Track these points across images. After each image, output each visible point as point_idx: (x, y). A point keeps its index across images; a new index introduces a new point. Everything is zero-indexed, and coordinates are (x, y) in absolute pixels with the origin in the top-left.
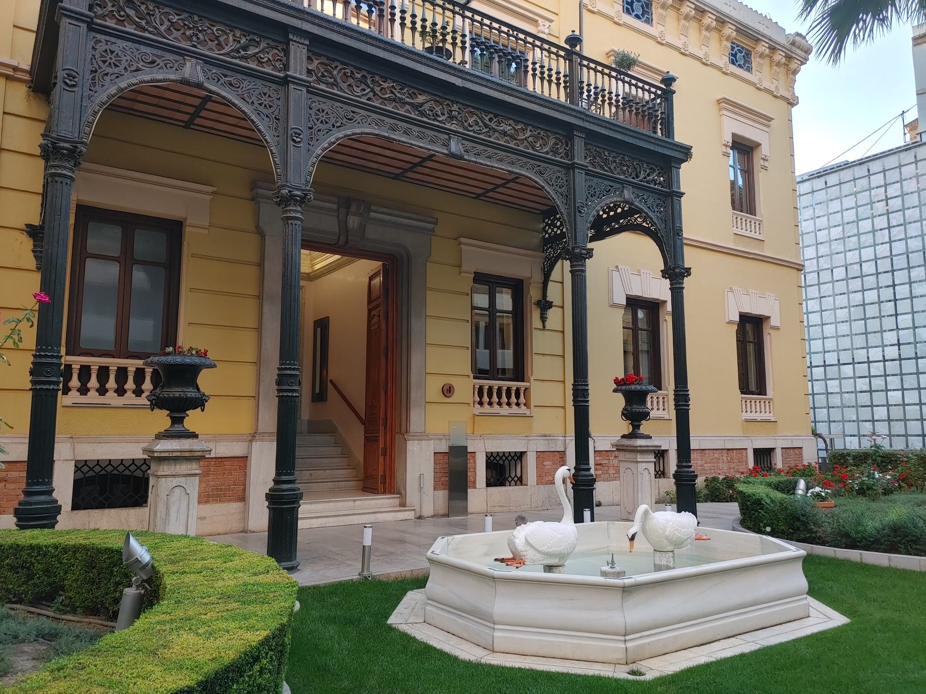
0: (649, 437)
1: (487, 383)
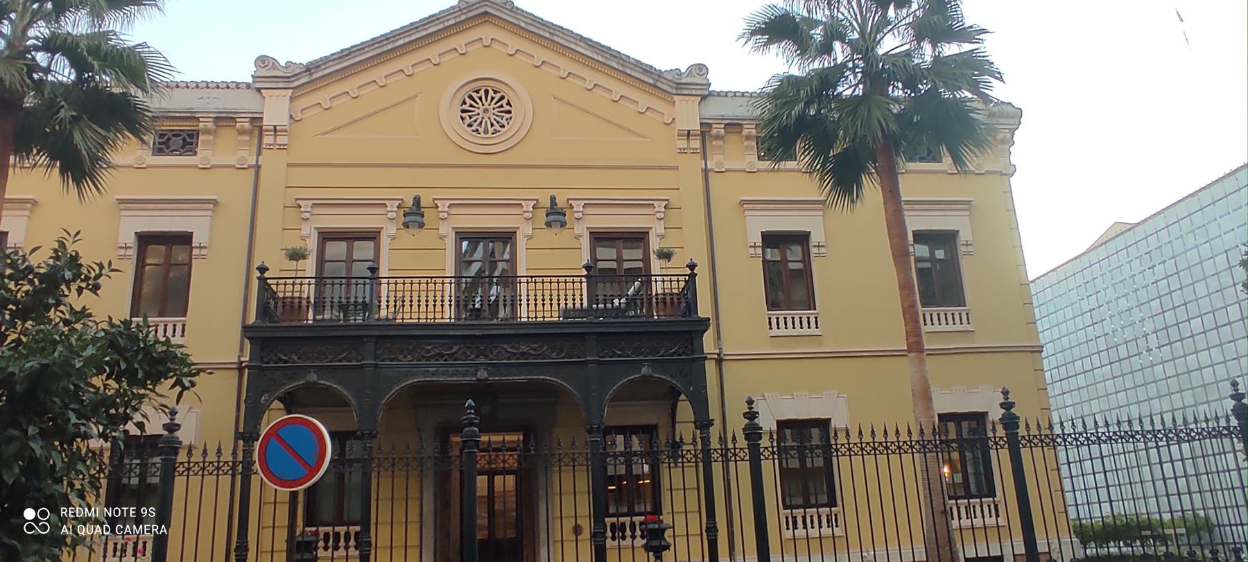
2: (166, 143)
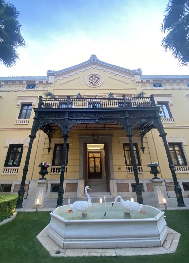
0: (159, 178)
1: (130, 167)
2: (29, 87)
